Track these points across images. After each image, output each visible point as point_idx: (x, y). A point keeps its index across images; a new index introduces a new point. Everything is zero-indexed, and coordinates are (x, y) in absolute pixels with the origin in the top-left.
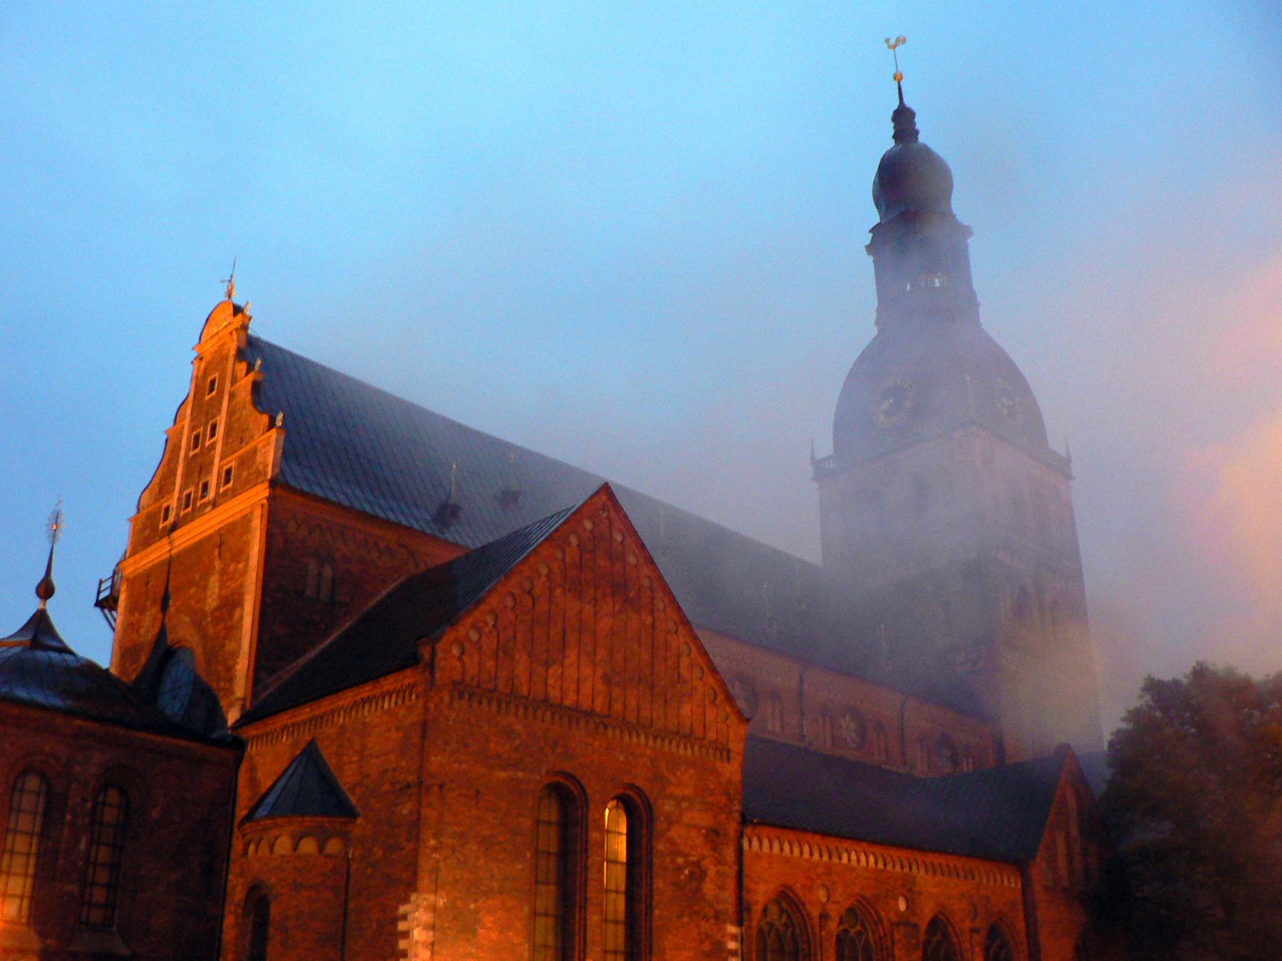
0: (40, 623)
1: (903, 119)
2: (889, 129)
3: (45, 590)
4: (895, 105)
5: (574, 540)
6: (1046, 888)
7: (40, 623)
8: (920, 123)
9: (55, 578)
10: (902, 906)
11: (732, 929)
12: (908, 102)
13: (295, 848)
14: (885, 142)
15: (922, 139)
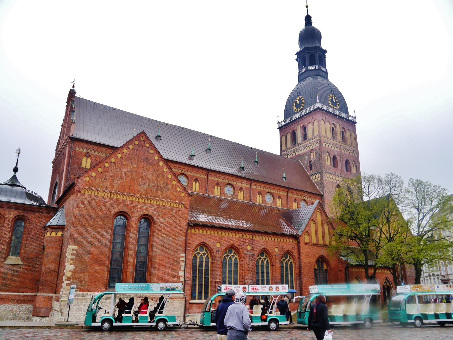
0: (14, 177)
1: (308, 19)
2: (304, 22)
3: (16, 170)
4: (306, 15)
5: (131, 147)
6: (306, 244)
7: (14, 177)
8: (313, 20)
9: (18, 167)
10: (249, 248)
11: (183, 255)
12: (309, 14)
13: (56, 234)
14: (302, 26)
15: (314, 25)
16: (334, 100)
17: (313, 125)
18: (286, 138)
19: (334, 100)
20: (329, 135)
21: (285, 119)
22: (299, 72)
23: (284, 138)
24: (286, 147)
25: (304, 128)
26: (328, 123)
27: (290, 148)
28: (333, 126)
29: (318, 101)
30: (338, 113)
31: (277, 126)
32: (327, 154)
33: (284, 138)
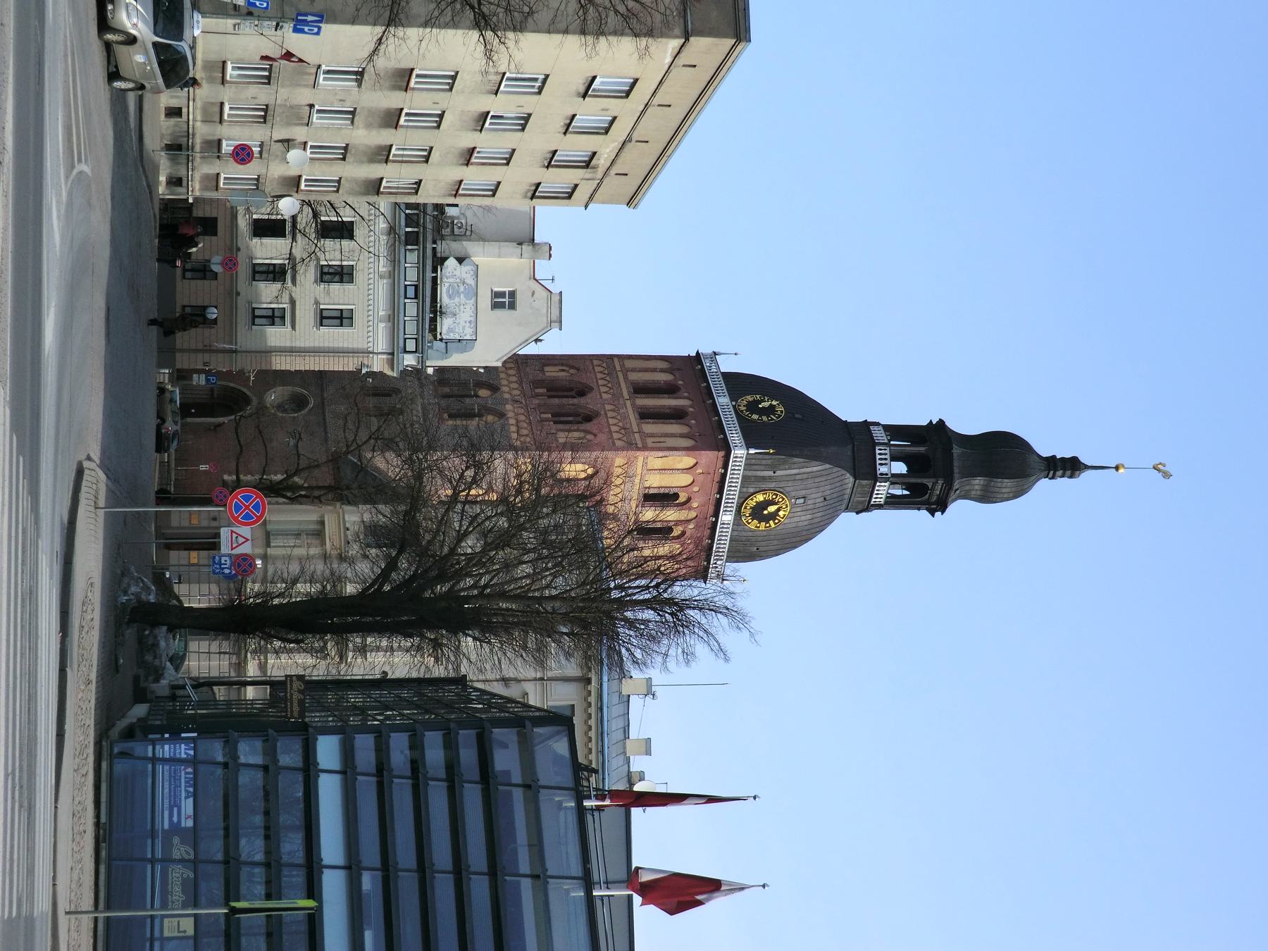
12: (1086, 475)
14: (1044, 448)
16: (772, 509)
17: (682, 436)
18: (662, 371)
19: (772, 509)
20: (656, 482)
21: (724, 374)
22: (877, 424)
23: (664, 365)
24: (634, 370)
25: (677, 415)
26: (685, 479)
27: (626, 378)
28: (682, 499)
29: (752, 451)
30: (726, 518)
31: (706, 350)
32: (590, 471)
33: (664, 365)
